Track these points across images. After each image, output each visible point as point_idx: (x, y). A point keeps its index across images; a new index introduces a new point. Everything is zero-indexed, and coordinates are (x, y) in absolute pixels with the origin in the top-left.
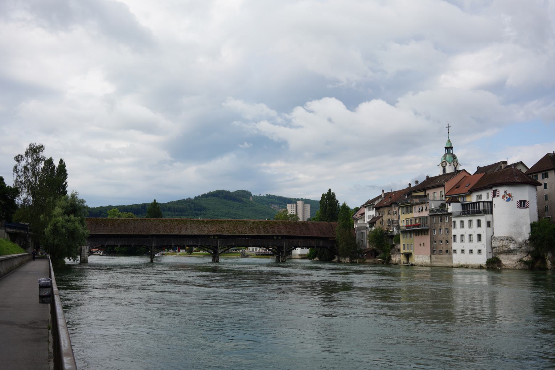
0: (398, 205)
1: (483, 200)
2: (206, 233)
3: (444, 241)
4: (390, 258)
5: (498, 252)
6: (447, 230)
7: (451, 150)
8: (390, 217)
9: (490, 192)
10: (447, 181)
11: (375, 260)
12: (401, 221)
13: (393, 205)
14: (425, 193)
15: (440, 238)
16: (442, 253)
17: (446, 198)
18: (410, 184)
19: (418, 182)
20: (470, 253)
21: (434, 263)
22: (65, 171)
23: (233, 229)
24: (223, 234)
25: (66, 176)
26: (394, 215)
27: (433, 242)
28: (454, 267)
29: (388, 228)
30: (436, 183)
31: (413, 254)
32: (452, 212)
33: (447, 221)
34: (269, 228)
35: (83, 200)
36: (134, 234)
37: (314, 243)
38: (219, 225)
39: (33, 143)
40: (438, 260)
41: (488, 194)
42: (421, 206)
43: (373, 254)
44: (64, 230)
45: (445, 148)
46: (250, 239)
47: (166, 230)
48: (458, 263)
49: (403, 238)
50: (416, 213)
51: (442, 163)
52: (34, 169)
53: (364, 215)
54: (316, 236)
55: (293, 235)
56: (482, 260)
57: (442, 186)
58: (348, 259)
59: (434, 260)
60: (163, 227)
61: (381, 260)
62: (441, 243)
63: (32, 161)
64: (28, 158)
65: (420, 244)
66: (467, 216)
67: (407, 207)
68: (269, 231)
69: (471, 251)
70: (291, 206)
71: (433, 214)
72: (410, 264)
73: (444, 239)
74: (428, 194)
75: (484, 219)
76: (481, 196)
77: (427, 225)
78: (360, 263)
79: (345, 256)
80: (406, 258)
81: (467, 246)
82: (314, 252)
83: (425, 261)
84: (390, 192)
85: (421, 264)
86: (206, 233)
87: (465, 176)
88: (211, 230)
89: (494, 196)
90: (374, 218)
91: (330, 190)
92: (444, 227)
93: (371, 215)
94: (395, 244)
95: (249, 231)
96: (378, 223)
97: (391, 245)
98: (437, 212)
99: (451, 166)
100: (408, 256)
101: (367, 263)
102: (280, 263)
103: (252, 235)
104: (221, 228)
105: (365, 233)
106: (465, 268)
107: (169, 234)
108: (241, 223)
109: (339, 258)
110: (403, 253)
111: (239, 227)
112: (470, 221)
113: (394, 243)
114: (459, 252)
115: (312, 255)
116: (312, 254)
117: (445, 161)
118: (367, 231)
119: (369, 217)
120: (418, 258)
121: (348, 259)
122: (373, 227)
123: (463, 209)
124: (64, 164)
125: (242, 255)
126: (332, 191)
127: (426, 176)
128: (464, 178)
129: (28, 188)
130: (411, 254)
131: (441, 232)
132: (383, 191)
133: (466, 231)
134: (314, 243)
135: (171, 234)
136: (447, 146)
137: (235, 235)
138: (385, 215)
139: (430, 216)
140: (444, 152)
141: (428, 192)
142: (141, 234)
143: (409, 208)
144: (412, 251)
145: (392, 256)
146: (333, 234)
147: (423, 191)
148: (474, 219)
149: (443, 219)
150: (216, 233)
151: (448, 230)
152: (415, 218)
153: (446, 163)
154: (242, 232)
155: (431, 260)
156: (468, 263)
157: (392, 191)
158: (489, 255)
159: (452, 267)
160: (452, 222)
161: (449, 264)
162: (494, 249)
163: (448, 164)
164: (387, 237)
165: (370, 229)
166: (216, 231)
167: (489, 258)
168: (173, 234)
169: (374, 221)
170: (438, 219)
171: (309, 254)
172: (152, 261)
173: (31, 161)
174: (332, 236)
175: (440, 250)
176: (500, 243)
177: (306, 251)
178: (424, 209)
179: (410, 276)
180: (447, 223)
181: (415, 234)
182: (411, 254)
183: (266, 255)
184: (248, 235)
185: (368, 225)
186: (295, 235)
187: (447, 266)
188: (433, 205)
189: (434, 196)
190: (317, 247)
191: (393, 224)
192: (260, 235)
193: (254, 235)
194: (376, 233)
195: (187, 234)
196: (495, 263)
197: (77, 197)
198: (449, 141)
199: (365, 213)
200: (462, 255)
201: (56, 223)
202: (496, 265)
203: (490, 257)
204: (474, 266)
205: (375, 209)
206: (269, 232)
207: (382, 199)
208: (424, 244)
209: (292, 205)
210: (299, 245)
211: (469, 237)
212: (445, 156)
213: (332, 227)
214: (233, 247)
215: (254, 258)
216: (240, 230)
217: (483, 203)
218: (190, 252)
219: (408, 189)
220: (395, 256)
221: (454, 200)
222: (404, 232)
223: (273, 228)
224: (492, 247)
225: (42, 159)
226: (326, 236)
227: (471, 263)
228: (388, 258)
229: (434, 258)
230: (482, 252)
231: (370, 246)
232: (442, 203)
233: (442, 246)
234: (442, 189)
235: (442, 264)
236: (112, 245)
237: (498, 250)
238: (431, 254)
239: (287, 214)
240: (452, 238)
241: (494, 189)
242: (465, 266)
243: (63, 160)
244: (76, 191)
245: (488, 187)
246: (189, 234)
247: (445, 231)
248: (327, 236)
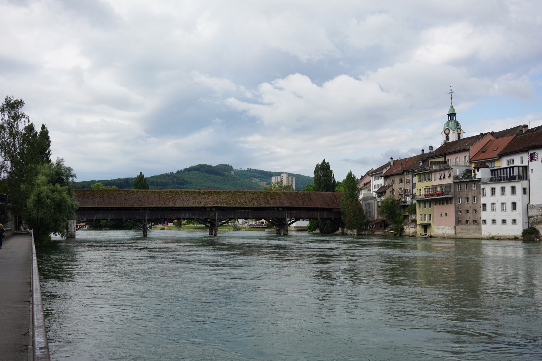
0: (413, 172)
1: (515, 164)
2: (203, 205)
3: (471, 211)
4: (402, 229)
5: (536, 221)
6: (475, 198)
7: (454, 116)
8: (402, 185)
9: (526, 157)
10: (472, 144)
11: (384, 232)
12: (418, 190)
13: (405, 173)
14: (445, 158)
15: (467, 207)
16: (468, 224)
17: (471, 163)
18: (423, 151)
19: (433, 148)
20: (502, 223)
21: (459, 235)
22: (48, 138)
23: (231, 201)
24: (221, 206)
25: (49, 143)
26: (406, 184)
27: (458, 211)
28: (483, 239)
29: (400, 197)
30: (457, 148)
31: (432, 225)
32: (480, 178)
33: (475, 189)
34: (269, 199)
35: (70, 168)
36: (125, 206)
37: (318, 215)
38: (216, 196)
39: (10, 96)
40: (464, 231)
41: (522, 158)
42: (442, 173)
43: (383, 225)
44: (49, 201)
45: (448, 114)
46: (250, 210)
47: (160, 202)
48: (488, 234)
49: (420, 208)
50: (436, 181)
51: (445, 130)
52: (11, 129)
53: (370, 184)
54: (320, 207)
55: (296, 206)
56: (518, 230)
57: (466, 150)
58: (355, 231)
59: (460, 231)
60: (157, 198)
61: (393, 232)
62: (468, 212)
63: (9, 118)
64: (4, 114)
65: (441, 214)
66: (499, 183)
67: (425, 174)
68: (270, 202)
69: (504, 221)
70: (276, 179)
71: (458, 182)
72: (429, 235)
73: (471, 208)
74: (448, 160)
75: (519, 186)
76: (513, 160)
77: (451, 193)
78: (368, 235)
79: (351, 229)
80: (424, 230)
81: (499, 215)
82: (315, 224)
83: (447, 232)
84: (399, 159)
85: (443, 236)
86: (203, 205)
87: (491, 140)
88: (209, 202)
89: (531, 160)
90: (382, 187)
91: (324, 160)
92: (471, 194)
93: (378, 185)
94: (408, 215)
95: (249, 202)
96: (388, 194)
97: (404, 216)
98: (462, 179)
99: (454, 134)
100: (426, 227)
101: (376, 235)
102: (282, 236)
103: (253, 206)
104: (219, 200)
105: (372, 203)
106: (497, 239)
107: (163, 206)
108: (240, 193)
109: (343, 230)
110: (420, 224)
111: (237, 198)
112: (503, 188)
113: (407, 214)
114: (489, 222)
115: (312, 228)
116: (313, 226)
117: (448, 129)
118: (374, 201)
119: (376, 186)
120: (438, 230)
121: (355, 231)
122: (382, 197)
123: (492, 175)
124: (47, 130)
125: (234, 228)
126: (326, 162)
127: (444, 141)
128: (490, 142)
129: (5, 151)
130: (430, 225)
131: (467, 200)
132: (392, 158)
133: (498, 199)
134: (317, 214)
135: (166, 206)
136: (450, 113)
137: (234, 207)
138: (396, 184)
139: (454, 183)
140: (446, 119)
141: (448, 158)
142: (133, 206)
143: (428, 175)
144: (430, 222)
145: (405, 227)
146: (337, 204)
147: (442, 157)
148: (508, 186)
149: (470, 187)
150: (214, 205)
151: (476, 199)
152: (435, 187)
153: (449, 130)
154: (241, 204)
155: (455, 231)
156: (500, 234)
157: (401, 159)
158: (525, 225)
159: (481, 239)
160: (481, 190)
161: (478, 236)
162: (531, 219)
163: (451, 131)
164: (399, 207)
165: (378, 199)
166: (213, 202)
167: (525, 228)
168: (168, 206)
169: (383, 190)
170: (464, 186)
171: (309, 226)
172: (145, 235)
173: (8, 118)
174: (337, 207)
175: (466, 221)
176: (539, 212)
177: (305, 223)
178: (447, 175)
179: (426, 248)
180: (474, 190)
181: (435, 204)
182: (430, 225)
183: (259, 228)
184: (248, 207)
185: (374, 195)
186: (298, 206)
187: (475, 238)
188: (458, 172)
189: (457, 162)
190: (320, 219)
191: (405, 193)
192: (261, 206)
193: (254, 206)
194: (387, 203)
195: (183, 206)
196: (533, 234)
197: (62, 165)
199: (371, 180)
200: (494, 226)
201: (39, 193)
202: (534, 236)
203: (526, 227)
204: (507, 238)
205: (383, 177)
206: (270, 203)
207: (391, 167)
208: (446, 214)
209: (277, 178)
210: (302, 217)
211: (502, 205)
212: (448, 123)
213: (336, 197)
214: (230, 219)
215: (247, 230)
216: (239, 201)
217: (517, 168)
218: (179, 226)
219: (421, 155)
220: (409, 227)
221: (481, 165)
222: (420, 202)
223: (274, 199)
224: (528, 217)
225: (21, 116)
226: (330, 207)
227: (504, 234)
228: (400, 230)
229: (459, 229)
230: (517, 221)
231: (378, 217)
232: (466, 169)
233: (469, 216)
234: (467, 154)
235: (468, 235)
236: (101, 218)
237: (536, 219)
238: (455, 224)
239: (282, 186)
240: (481, 207)
241: (530, 152)
242: (497, 238)
243: (45, 126)
244: (62, 158)
245: (524, 150)
246: (185, 206)
247: (472, 200)
248: (331, 207)
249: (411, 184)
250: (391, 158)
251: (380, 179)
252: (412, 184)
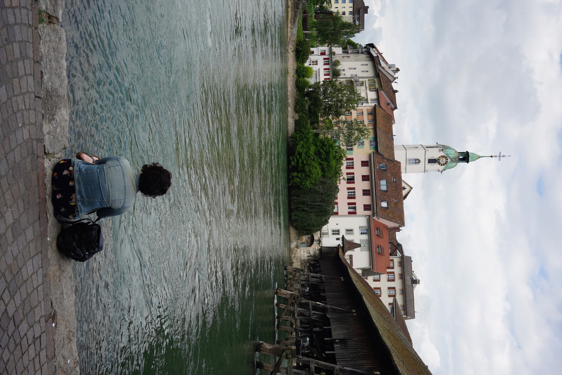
51: (446, 158)
117: (447, 162)
136: (470, 155)
153: (444, 165)
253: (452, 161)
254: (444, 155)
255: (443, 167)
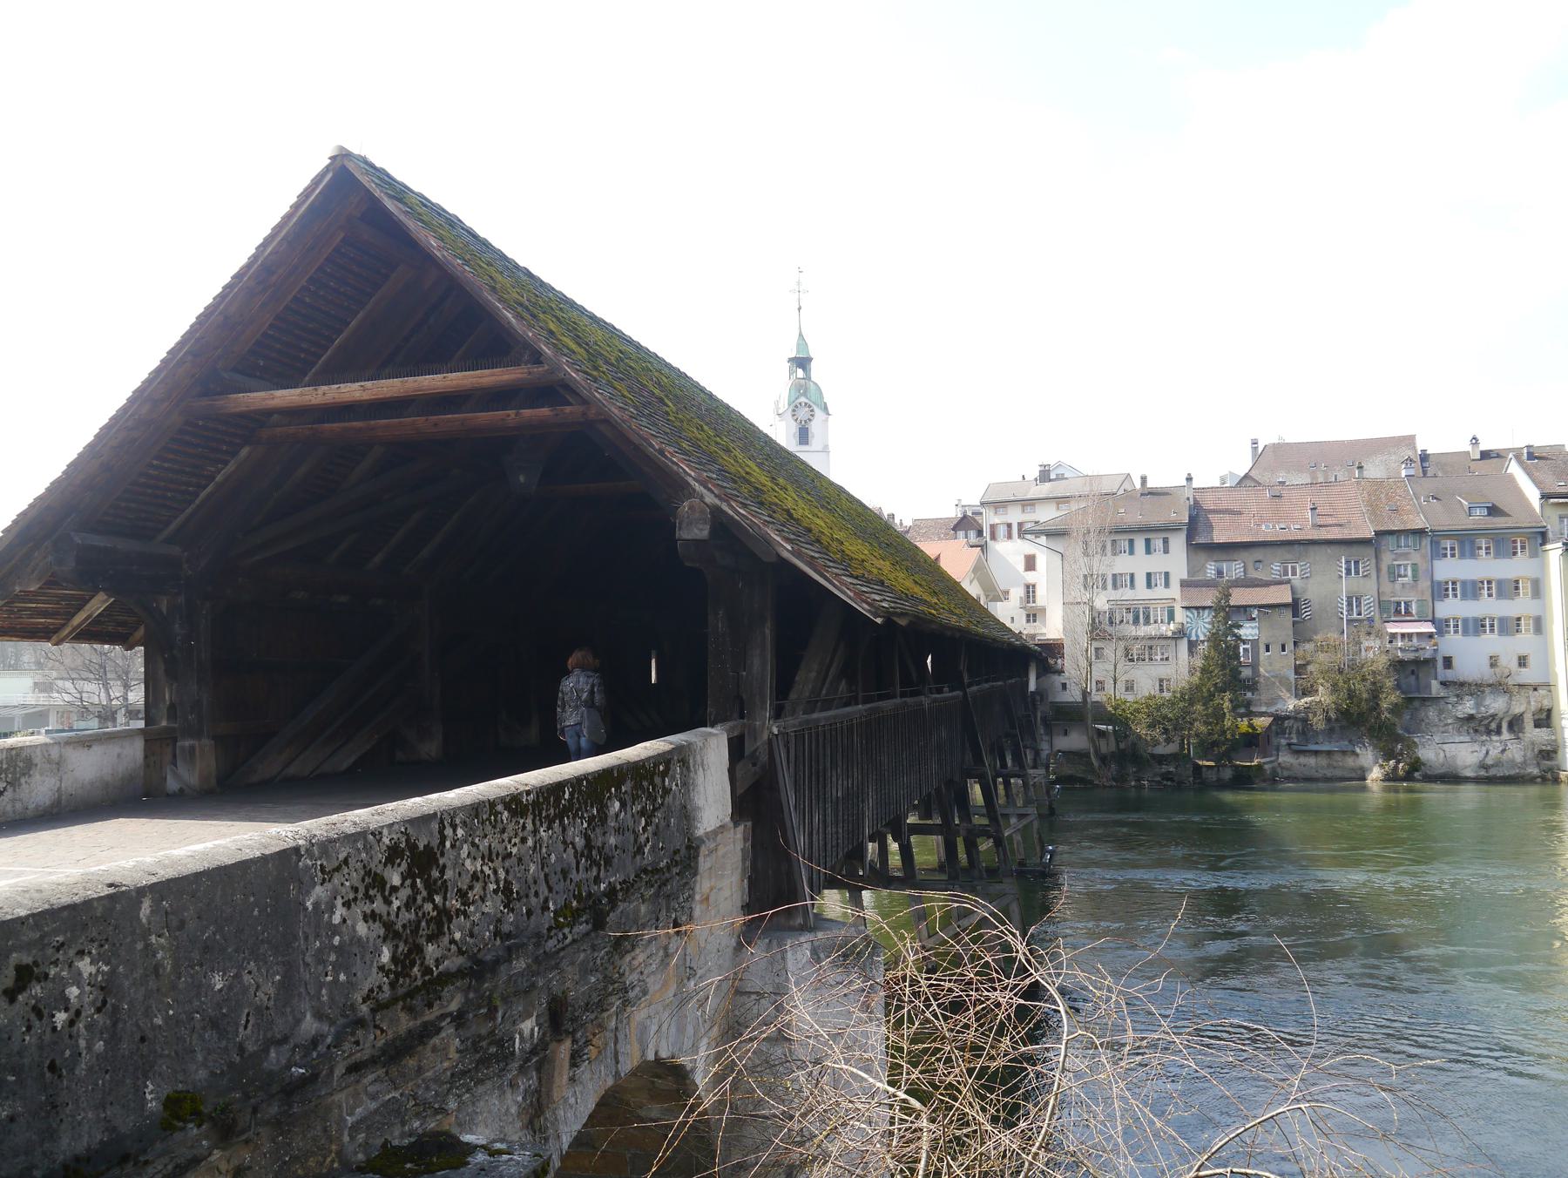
51: (796, 406)
117: (806, 404)
132: (1189, 479)
153: (812, 411)
198: (801, 335)
249: (1425, 584)
250: (1186, 476)
251: (1148, 551)
252: (1429, 583)
253: (805, 394)
254: (790, 410)
255: (818, 413)
